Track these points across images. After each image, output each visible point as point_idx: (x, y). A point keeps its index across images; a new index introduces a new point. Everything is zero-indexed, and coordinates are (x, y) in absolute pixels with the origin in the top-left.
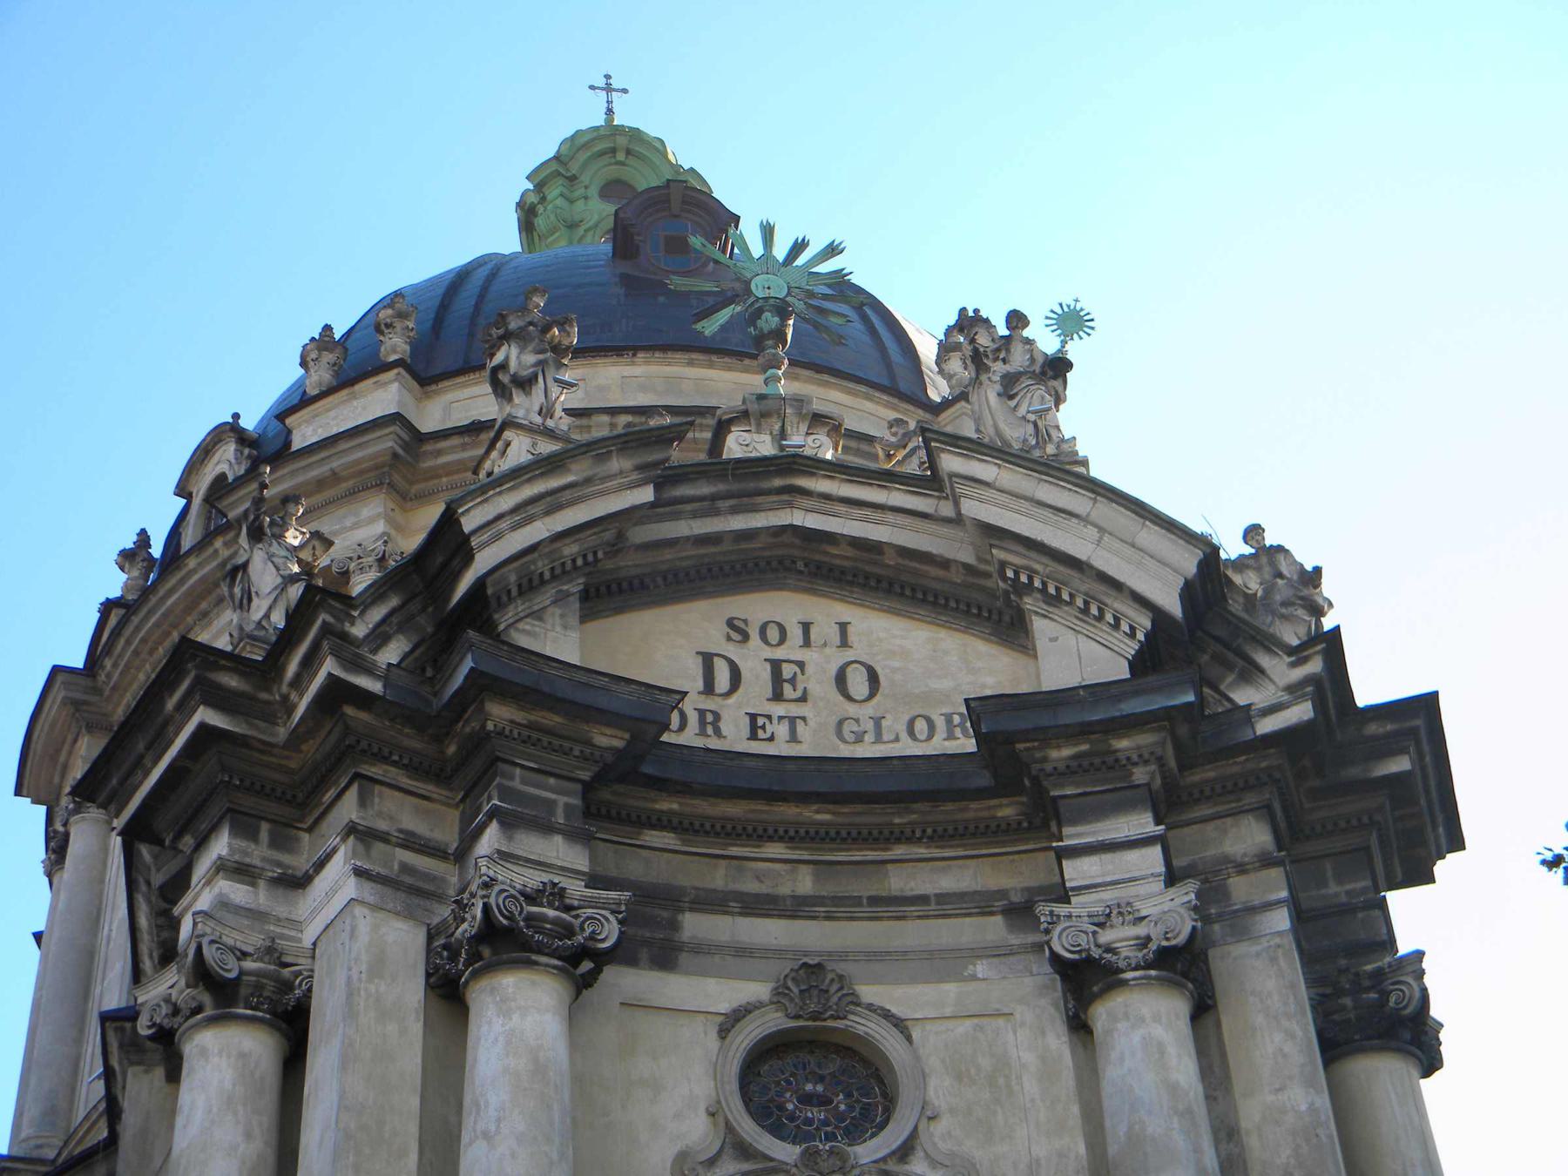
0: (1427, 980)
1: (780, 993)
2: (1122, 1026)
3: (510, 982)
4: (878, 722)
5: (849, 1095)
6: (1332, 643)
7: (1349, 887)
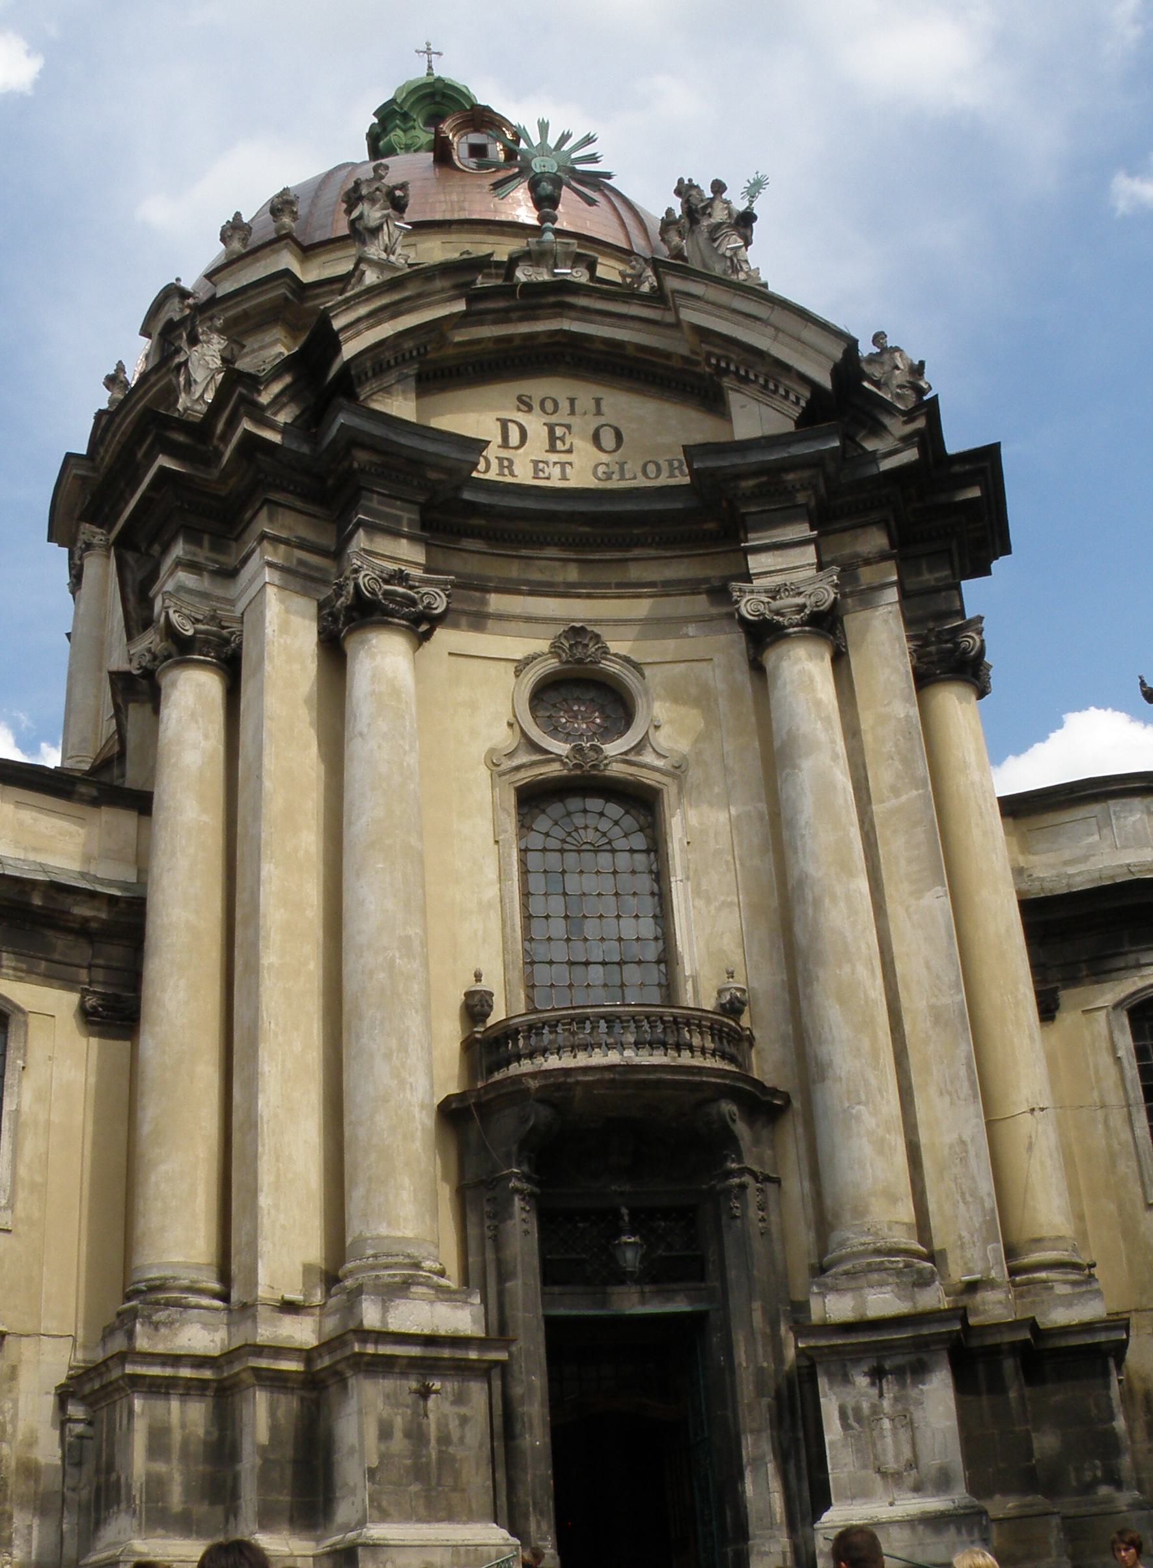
2: (785, 664)
4: (622, 466)
6: (930, 409)
7: (936, 575)
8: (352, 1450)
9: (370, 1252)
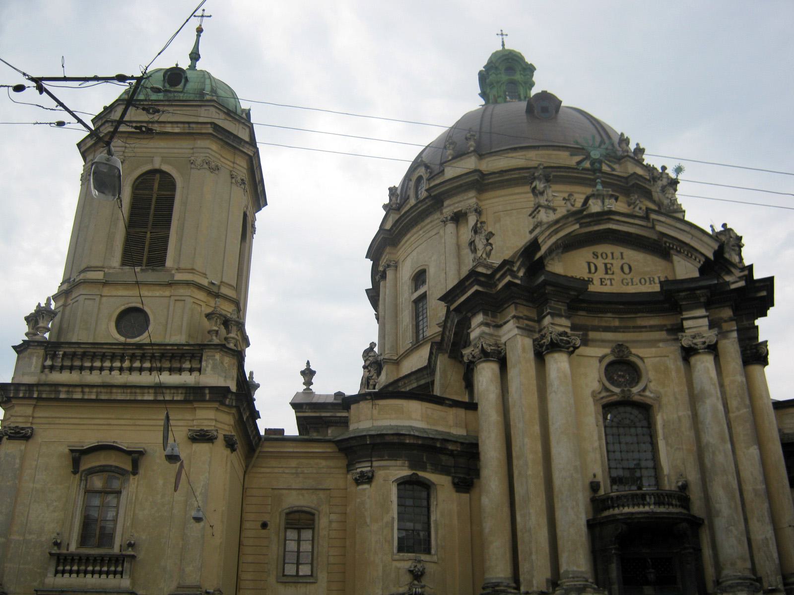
0: (768, 347)
1: (613, 351)
2: (699, 363)
3: (556, 355)
4: (632, 280)
5: (629, 375)
9: (571, 576)
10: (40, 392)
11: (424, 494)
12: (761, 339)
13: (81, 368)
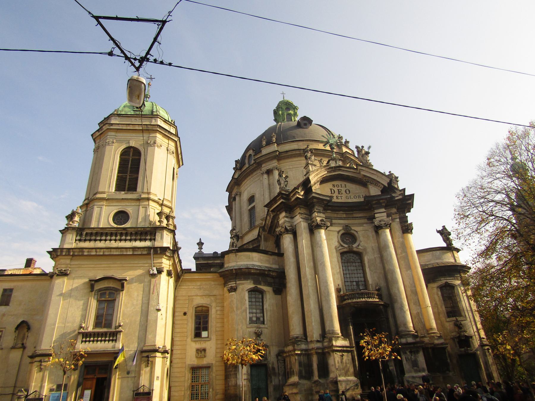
1: (343, 229)
8: (333, 365)
10: (74, 252)
11: (260, 296)
12: (409, 222)
13: (95, 240)
